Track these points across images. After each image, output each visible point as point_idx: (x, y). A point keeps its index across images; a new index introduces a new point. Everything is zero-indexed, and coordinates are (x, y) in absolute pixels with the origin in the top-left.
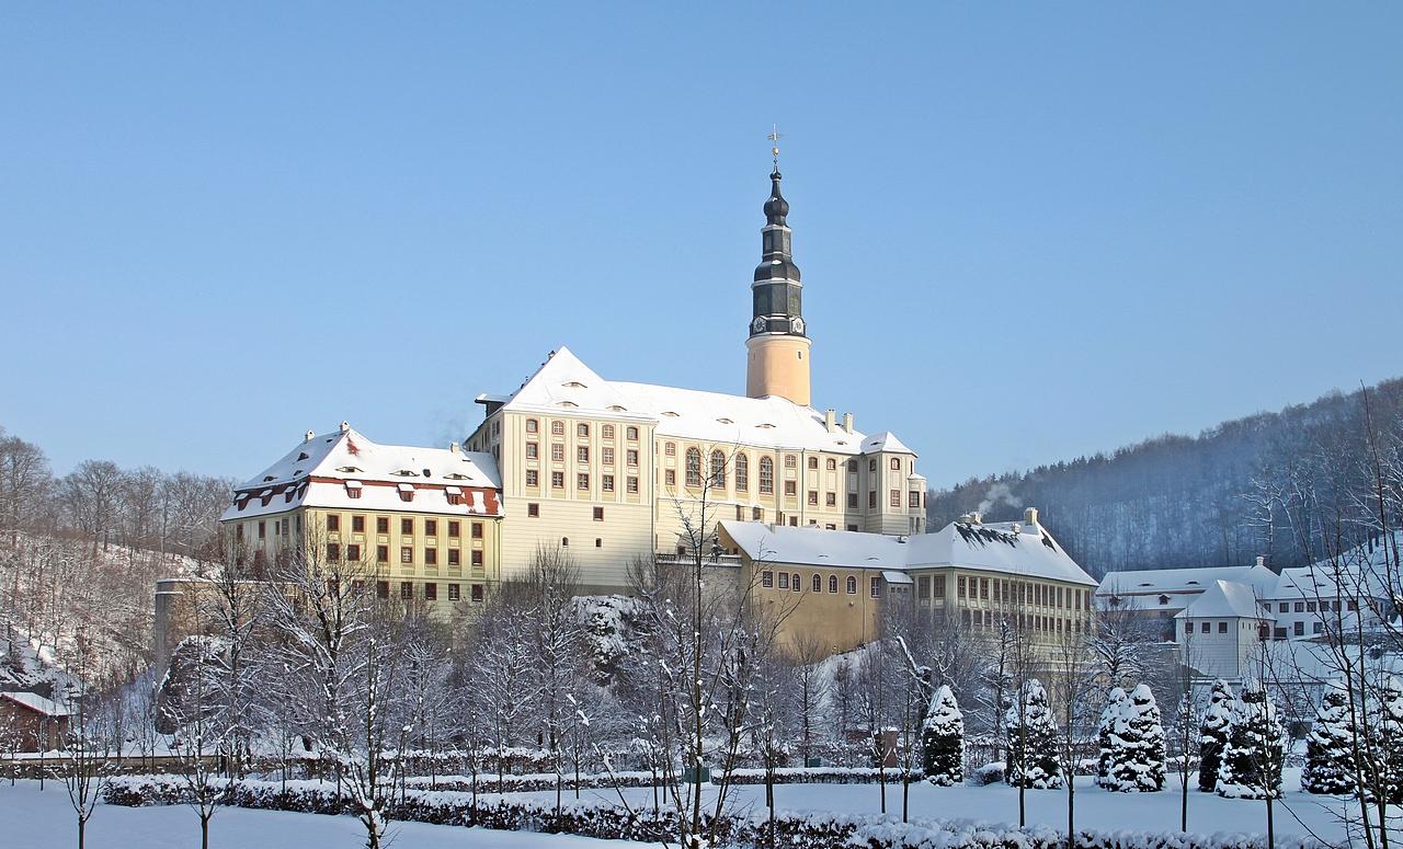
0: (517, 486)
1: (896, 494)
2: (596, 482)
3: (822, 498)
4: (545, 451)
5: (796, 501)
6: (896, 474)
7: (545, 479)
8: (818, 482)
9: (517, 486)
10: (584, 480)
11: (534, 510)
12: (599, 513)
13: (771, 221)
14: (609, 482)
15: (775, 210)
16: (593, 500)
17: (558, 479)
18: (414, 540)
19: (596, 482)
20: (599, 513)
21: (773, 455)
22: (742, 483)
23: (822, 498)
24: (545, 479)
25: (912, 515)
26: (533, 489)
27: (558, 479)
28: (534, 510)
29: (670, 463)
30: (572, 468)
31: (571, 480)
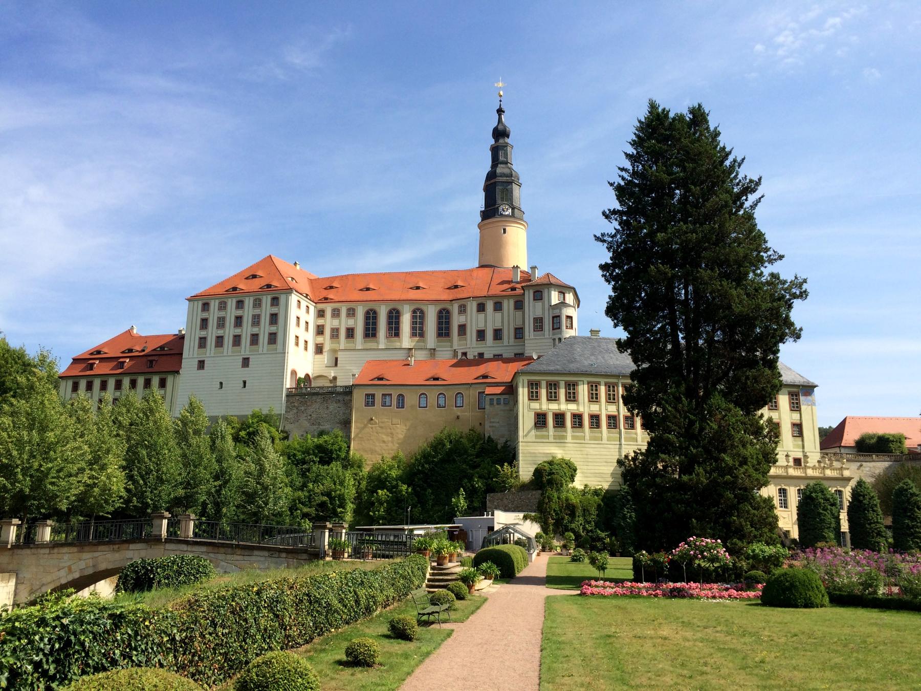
0: (191, 350)
1: (539, 324)
2: (246, 341)
3: (489, 335)
4: (213, 322)
5: (466, 340)
6: (539, 304)
7: (211, 342)
8: (486, 322)
9: (191, 350)
10: (237, 340)
11: (201, 365)
12: (246, 362)
13: (496, 141)
14: (255, 339)
15: (500, 133)
16: (243, 353)
17: (220, 341)
19: (246, 341)
20: (246, 362)
21: (448, 306)
22: (418, 330)
23: (489, 335)
24: (211, 342)
25: (554, 337)
26: (202, 350)
27: (220, 341)
28: (201, 365)
29: (351, 323)
30: (229, 332)
31: (228, 341)
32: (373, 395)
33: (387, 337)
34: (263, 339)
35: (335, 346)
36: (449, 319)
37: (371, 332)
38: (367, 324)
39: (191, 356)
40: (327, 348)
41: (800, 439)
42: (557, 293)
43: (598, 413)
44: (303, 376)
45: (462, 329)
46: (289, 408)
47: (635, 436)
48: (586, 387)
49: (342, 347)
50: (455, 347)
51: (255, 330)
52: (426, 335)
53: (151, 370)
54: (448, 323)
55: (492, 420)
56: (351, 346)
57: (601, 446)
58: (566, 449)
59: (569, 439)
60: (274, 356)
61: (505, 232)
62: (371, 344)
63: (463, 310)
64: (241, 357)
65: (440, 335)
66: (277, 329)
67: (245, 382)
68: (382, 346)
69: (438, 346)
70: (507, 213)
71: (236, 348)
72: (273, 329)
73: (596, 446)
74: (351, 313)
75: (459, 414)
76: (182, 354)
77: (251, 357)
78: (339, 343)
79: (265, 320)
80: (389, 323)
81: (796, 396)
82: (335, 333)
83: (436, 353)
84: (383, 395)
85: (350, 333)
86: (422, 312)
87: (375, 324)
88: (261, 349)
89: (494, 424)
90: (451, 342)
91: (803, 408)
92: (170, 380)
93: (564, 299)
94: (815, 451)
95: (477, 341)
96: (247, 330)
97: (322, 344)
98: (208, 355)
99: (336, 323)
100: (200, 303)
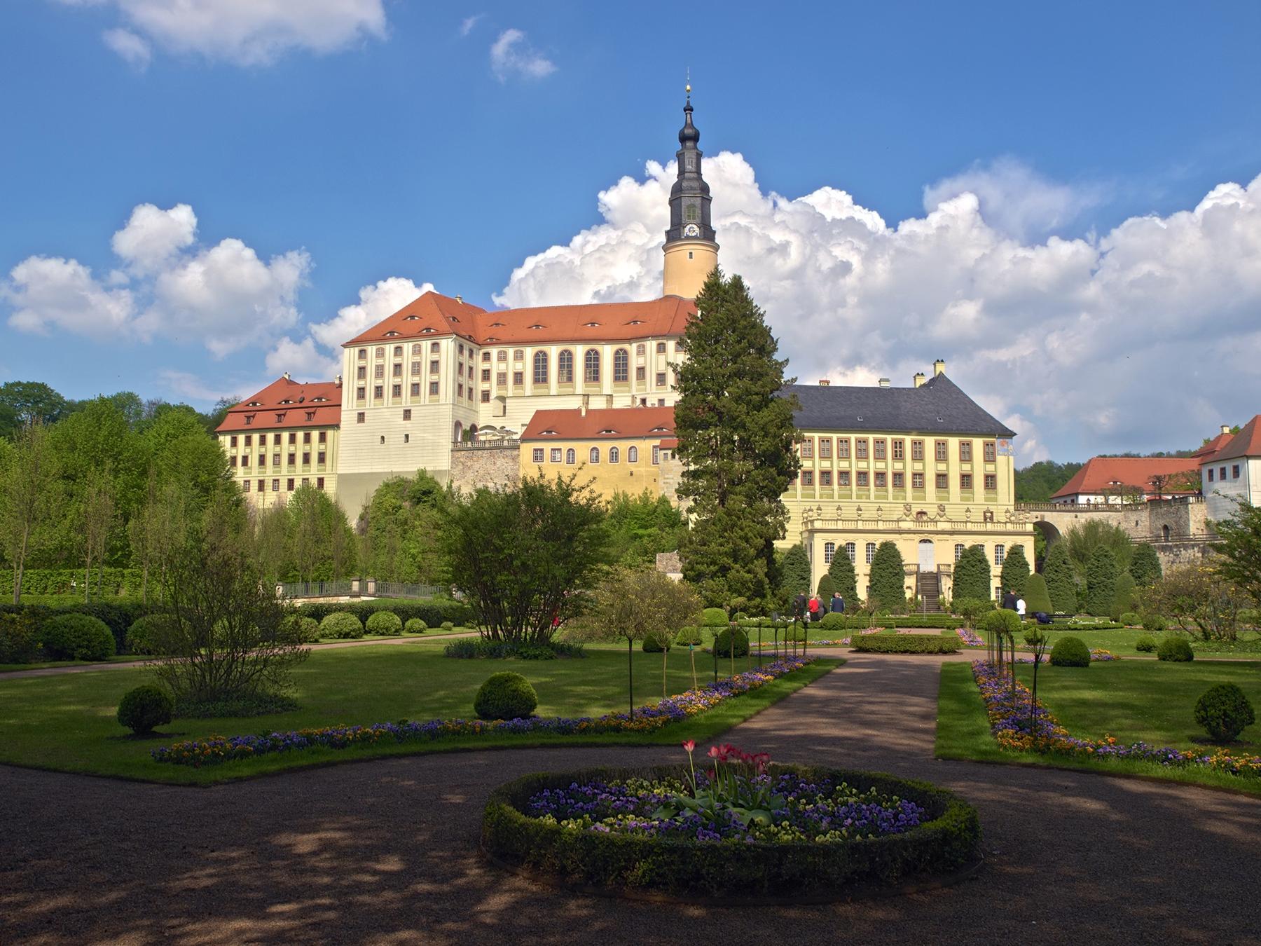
2: (406, 391)
4: (371, 371)
5: (645, 385)
7: (370, 393)
10: (397, 390)
11: (361, 418)
12: (407, 414)
14: (415, 388)
16: (404, 404)
17: (379, 391)
18: (281, 449)
19: (406, 391)
20: (407, 414)
24: (370, 393)
26: (362, 401)
27: (379, 391)
28: (361, 418)
29: (519, 367)
30: (389, 381)
31: (388, 391)
32: (542, 450)
33: (559, 382)
34: (425, 389)
35: (503, 393)
36: (626, 360)
37: (541, 376)
38: (536, 368)
39: (350, 408)
40: (493, 395)
44: (468, 429)
45: (641, 371)
46: (455, 462)
47: (813, 492)
49: (510, 394)
50: (634, 393)
51: (416, 379)
52: (601, 379)
53: (309, 423)
54: (626, 365)
55: (666, 476)
56: (520, 392)
60: (437, 407)
61: (691, 257)
62: (543, 391)
63: (642, 351)
64: (402, 409)
65: (616, 379)
66: (439, 378)
67: (407, 436)
68: (553, 392)
69: (615, 392)
70: (694, 234)
71: (397, 399)
72: (435, 378)
74: (519, 356)
75: (633, 469)
76: (340, 405)
77: (412, 408)
78: (506, 389)
79: (426, 367)
80: (561, 367)
81: (992, 445)
82: (502, 378)
83: (614, 399)
84: (552, 449)
85: (519, 377)
86: (597, 353)
87: (545, 367)
88: (422, 399)
89: (668, 481)
90: (629, 386)
91: (999, 458)
92: (330, 433)
94: (1008, 503)
95: (657, 385)
96: (407, 380)
97: (488, 391)
98: (368, 407)
99: (502, 367)
100: (357, 349)
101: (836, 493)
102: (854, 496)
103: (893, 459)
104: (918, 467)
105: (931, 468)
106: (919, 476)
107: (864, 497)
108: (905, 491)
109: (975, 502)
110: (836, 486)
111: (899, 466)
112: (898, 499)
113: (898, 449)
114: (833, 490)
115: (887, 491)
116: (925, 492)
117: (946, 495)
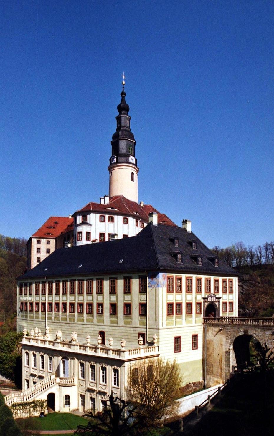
41: (144, 317)
42: (81, 217)
43: (38, 301)
47: (51, 316)
48: (35, 284)
57: (39, 322)
58: (28, 324)
59: (29, 319)
73: (37, 322)
91: (149, 289)
93: (86, 220)
94: (155, 327)
101: (60, 317)
102: (68, 319)
103: (87, 294)
104: (100, 298)
105: (107, 299)
106: (100, 305)
107: (72, 320)
108: (93, 316)
109: (134, 326)
110: (60, 313)
111: (90, 298)
112: (89, 322)
113: (89, 286)
114: (59, 315)
115: (83, 316)
116: (104, 317)
117: (114, 319)
